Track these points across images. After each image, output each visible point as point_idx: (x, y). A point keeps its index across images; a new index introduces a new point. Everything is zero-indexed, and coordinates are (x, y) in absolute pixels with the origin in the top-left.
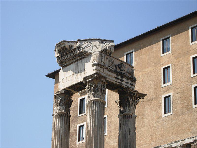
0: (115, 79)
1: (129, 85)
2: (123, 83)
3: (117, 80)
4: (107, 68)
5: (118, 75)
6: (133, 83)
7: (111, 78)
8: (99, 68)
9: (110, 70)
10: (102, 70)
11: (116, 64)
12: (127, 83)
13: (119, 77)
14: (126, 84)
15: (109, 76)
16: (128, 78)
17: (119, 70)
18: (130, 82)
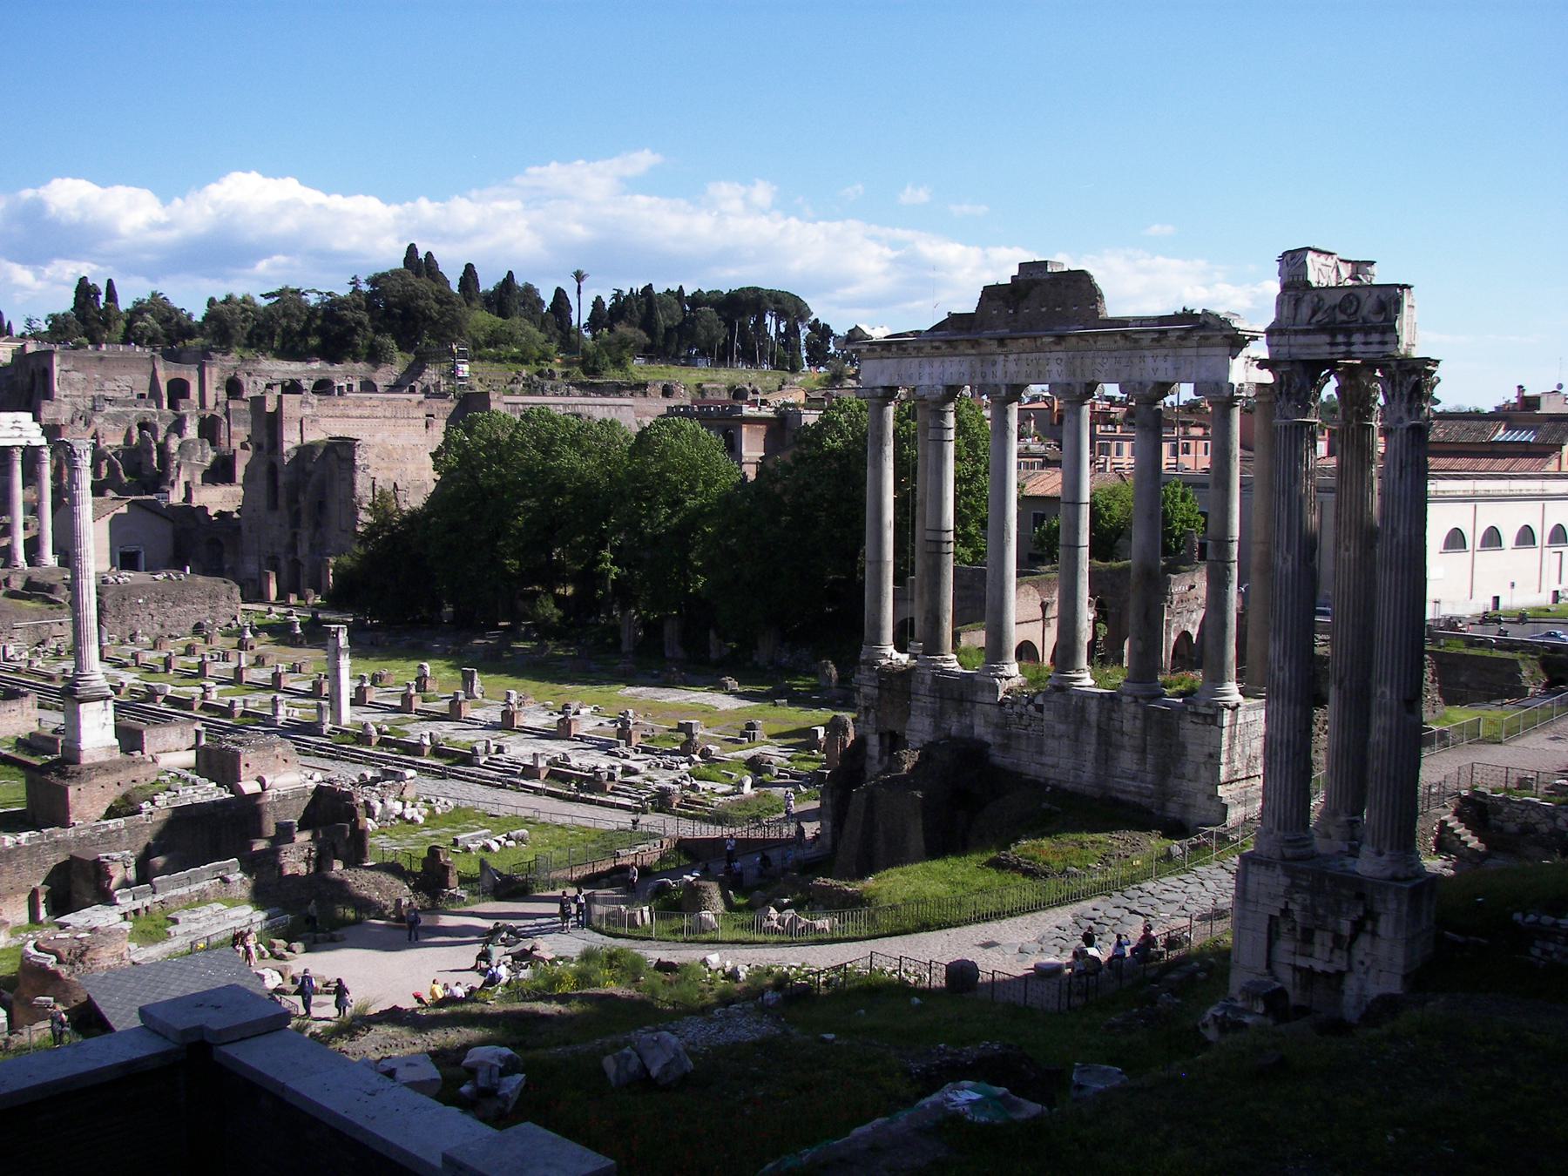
0: (1328, 349)
1: (1375, 348)
2: (1354, 349)
3: (1334, 349)
4: (1296, 332)
5: (1333, 336)
6: (1388, 338)
7: (1314, 350)
8: (1275, 339)
9: (1307, 332)
10: (1284, 340)
11: (1333, 303)
12: (1366, 344)
13: (1340, 339)
14: (1363, 348)
15: (1308, 346)
16: (1367, 330)
17: (1342, 317)
18: (1375, 337)
